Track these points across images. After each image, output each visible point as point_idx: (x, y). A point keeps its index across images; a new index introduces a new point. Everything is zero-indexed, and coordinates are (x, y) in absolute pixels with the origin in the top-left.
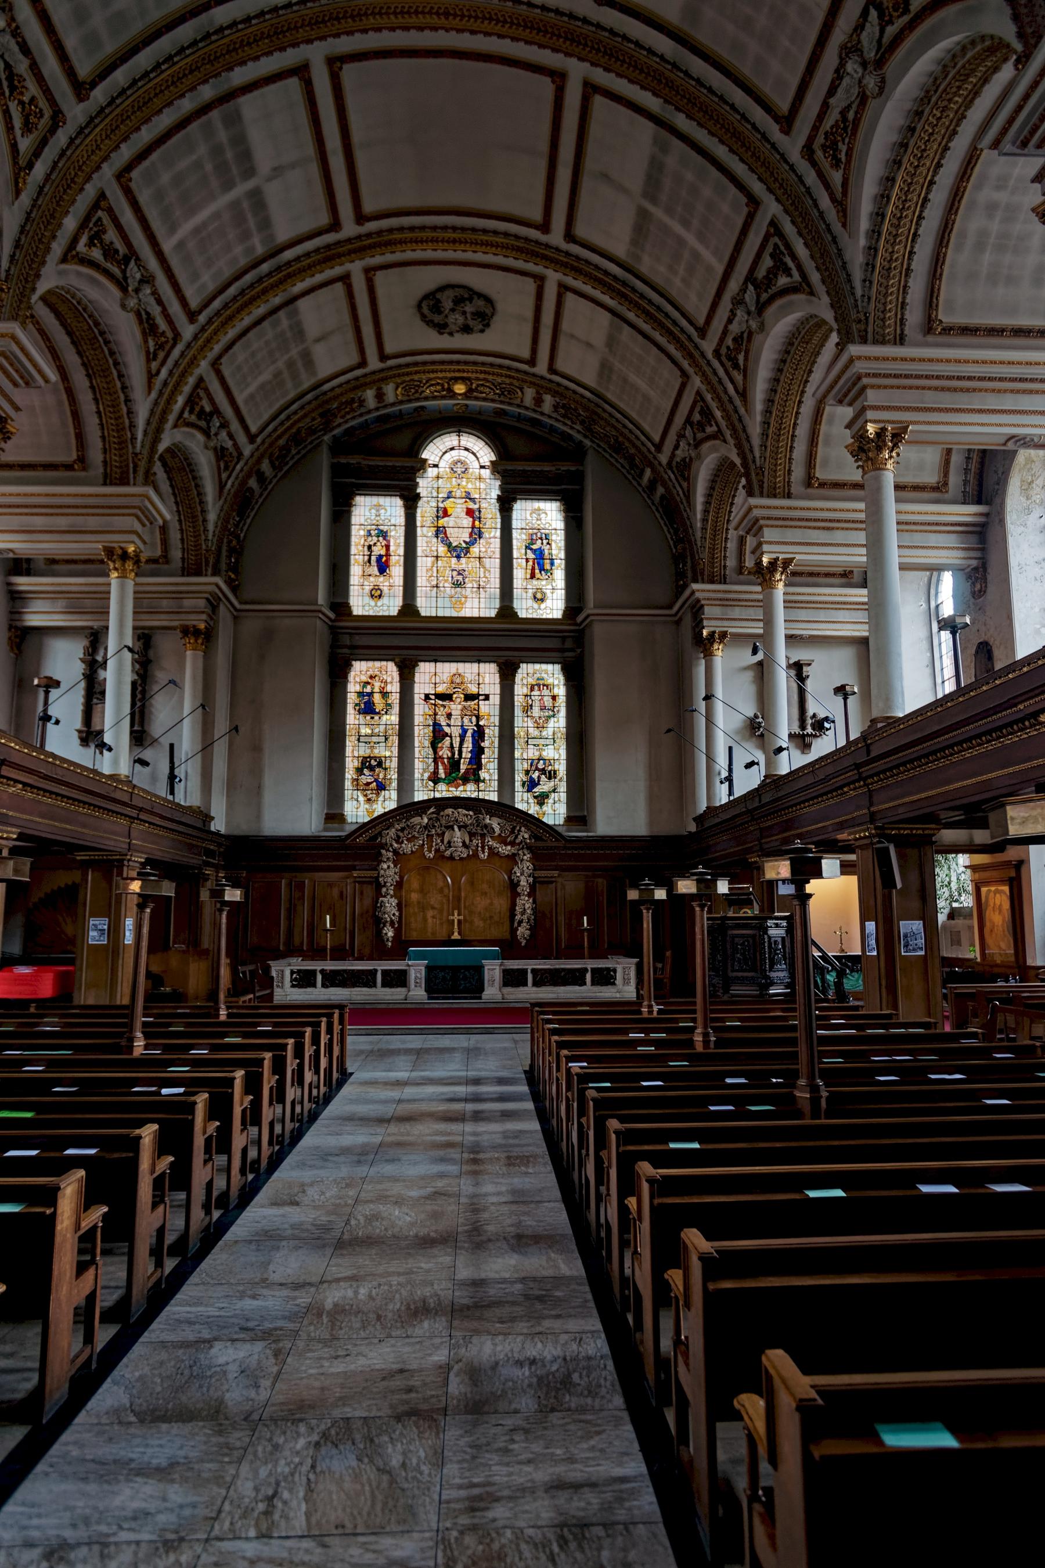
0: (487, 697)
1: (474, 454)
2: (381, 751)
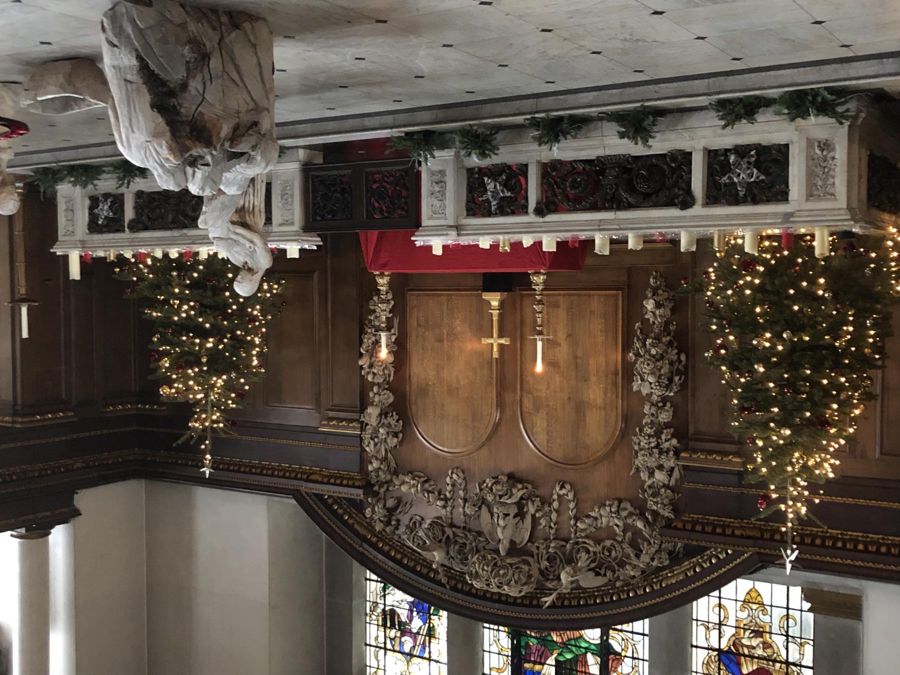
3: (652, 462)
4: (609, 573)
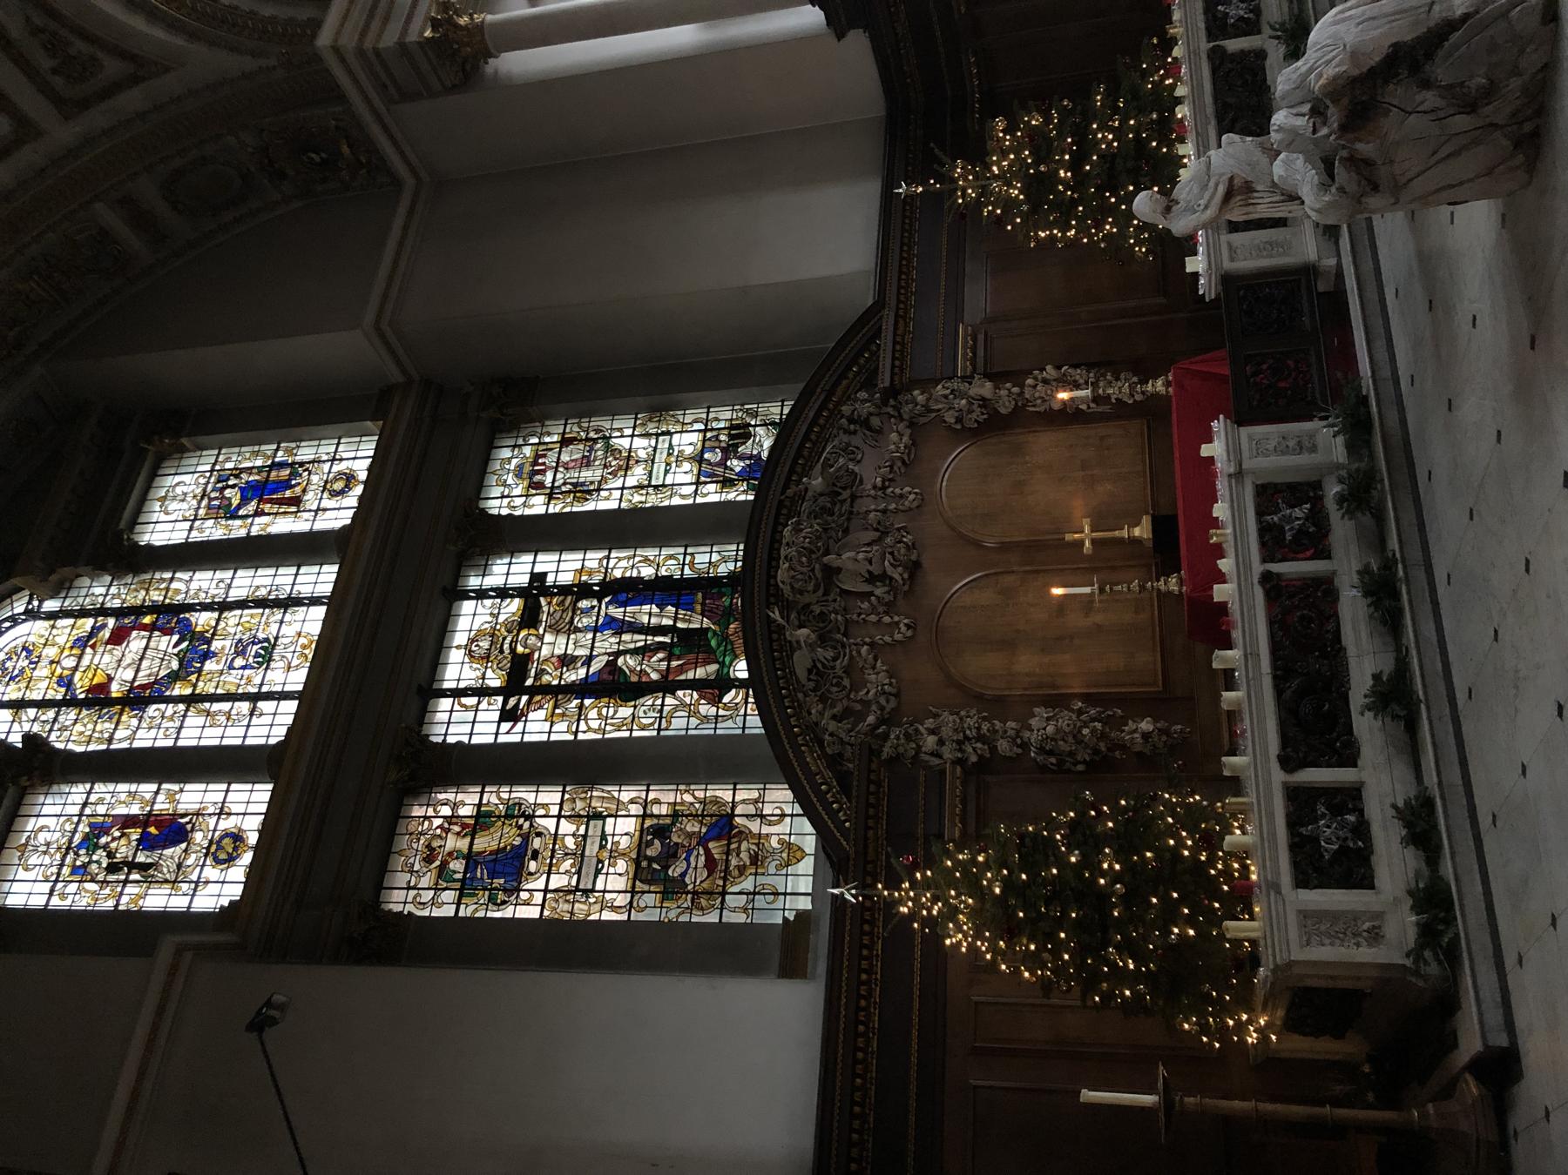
0: (538, 578)
2: (623, 829)
3: (946, 732)
4: (812, 685)
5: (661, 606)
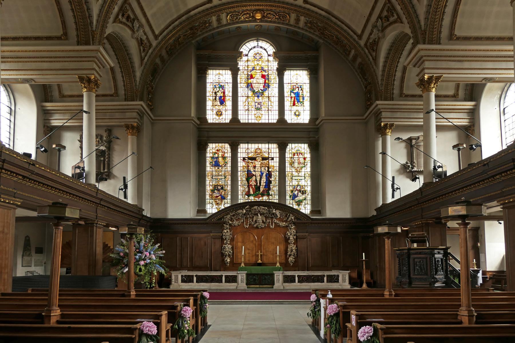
0: (273, 159)
1: (265, 50)
5: (265, 182)
